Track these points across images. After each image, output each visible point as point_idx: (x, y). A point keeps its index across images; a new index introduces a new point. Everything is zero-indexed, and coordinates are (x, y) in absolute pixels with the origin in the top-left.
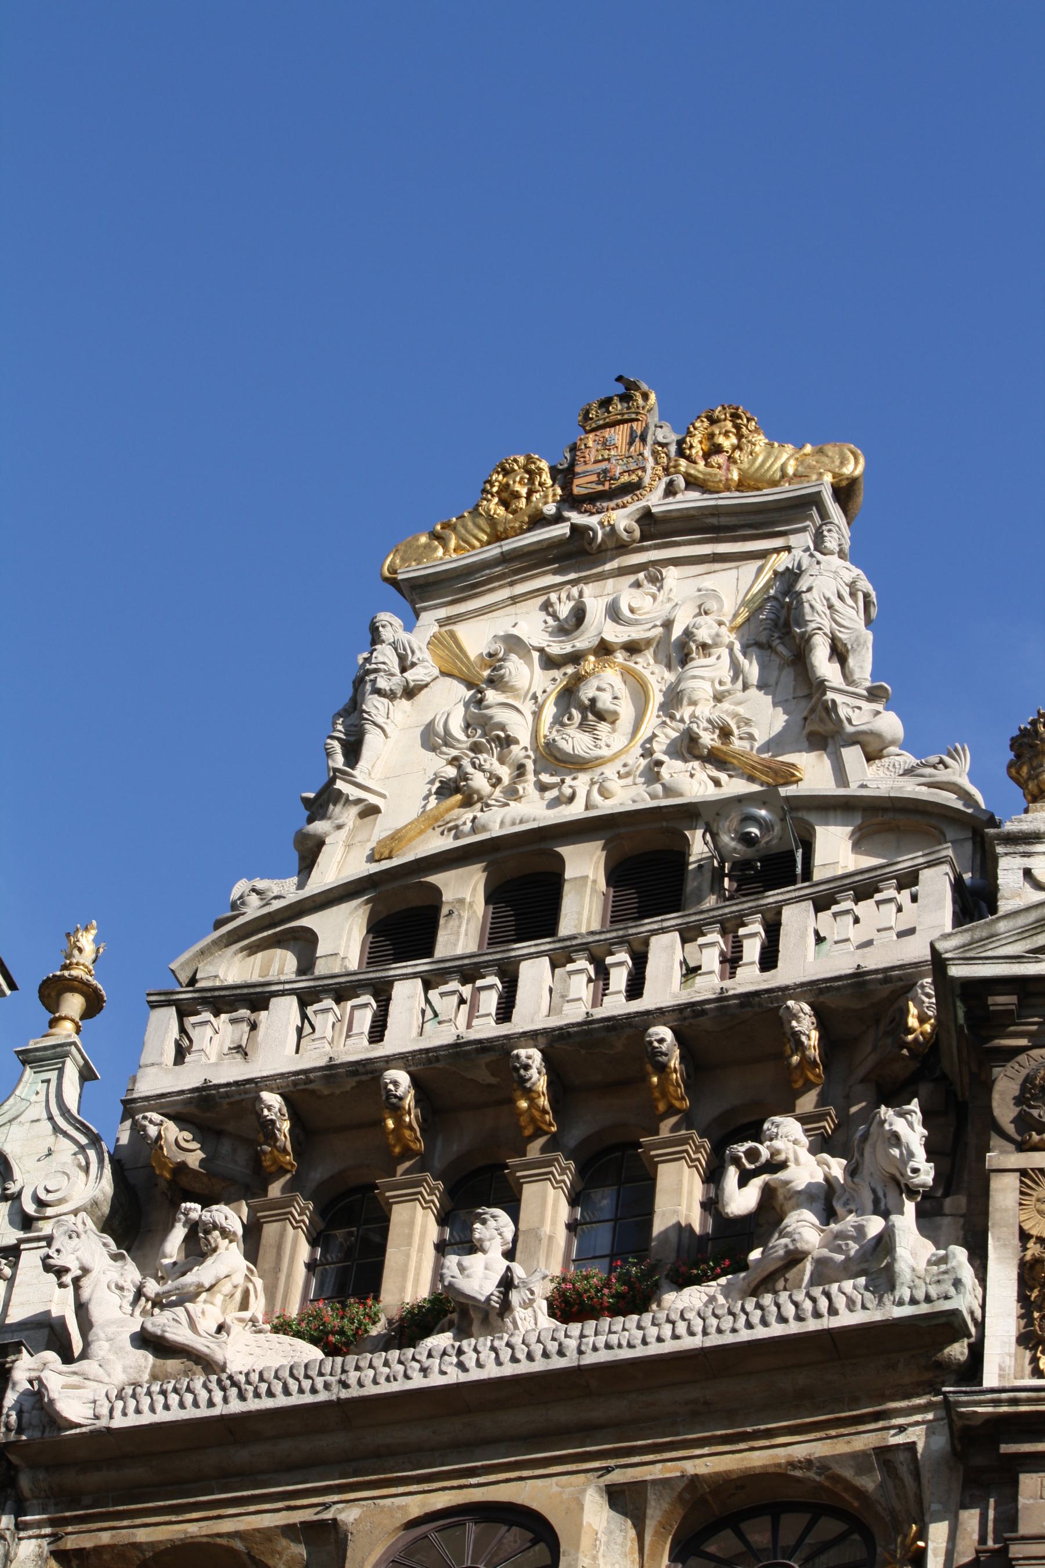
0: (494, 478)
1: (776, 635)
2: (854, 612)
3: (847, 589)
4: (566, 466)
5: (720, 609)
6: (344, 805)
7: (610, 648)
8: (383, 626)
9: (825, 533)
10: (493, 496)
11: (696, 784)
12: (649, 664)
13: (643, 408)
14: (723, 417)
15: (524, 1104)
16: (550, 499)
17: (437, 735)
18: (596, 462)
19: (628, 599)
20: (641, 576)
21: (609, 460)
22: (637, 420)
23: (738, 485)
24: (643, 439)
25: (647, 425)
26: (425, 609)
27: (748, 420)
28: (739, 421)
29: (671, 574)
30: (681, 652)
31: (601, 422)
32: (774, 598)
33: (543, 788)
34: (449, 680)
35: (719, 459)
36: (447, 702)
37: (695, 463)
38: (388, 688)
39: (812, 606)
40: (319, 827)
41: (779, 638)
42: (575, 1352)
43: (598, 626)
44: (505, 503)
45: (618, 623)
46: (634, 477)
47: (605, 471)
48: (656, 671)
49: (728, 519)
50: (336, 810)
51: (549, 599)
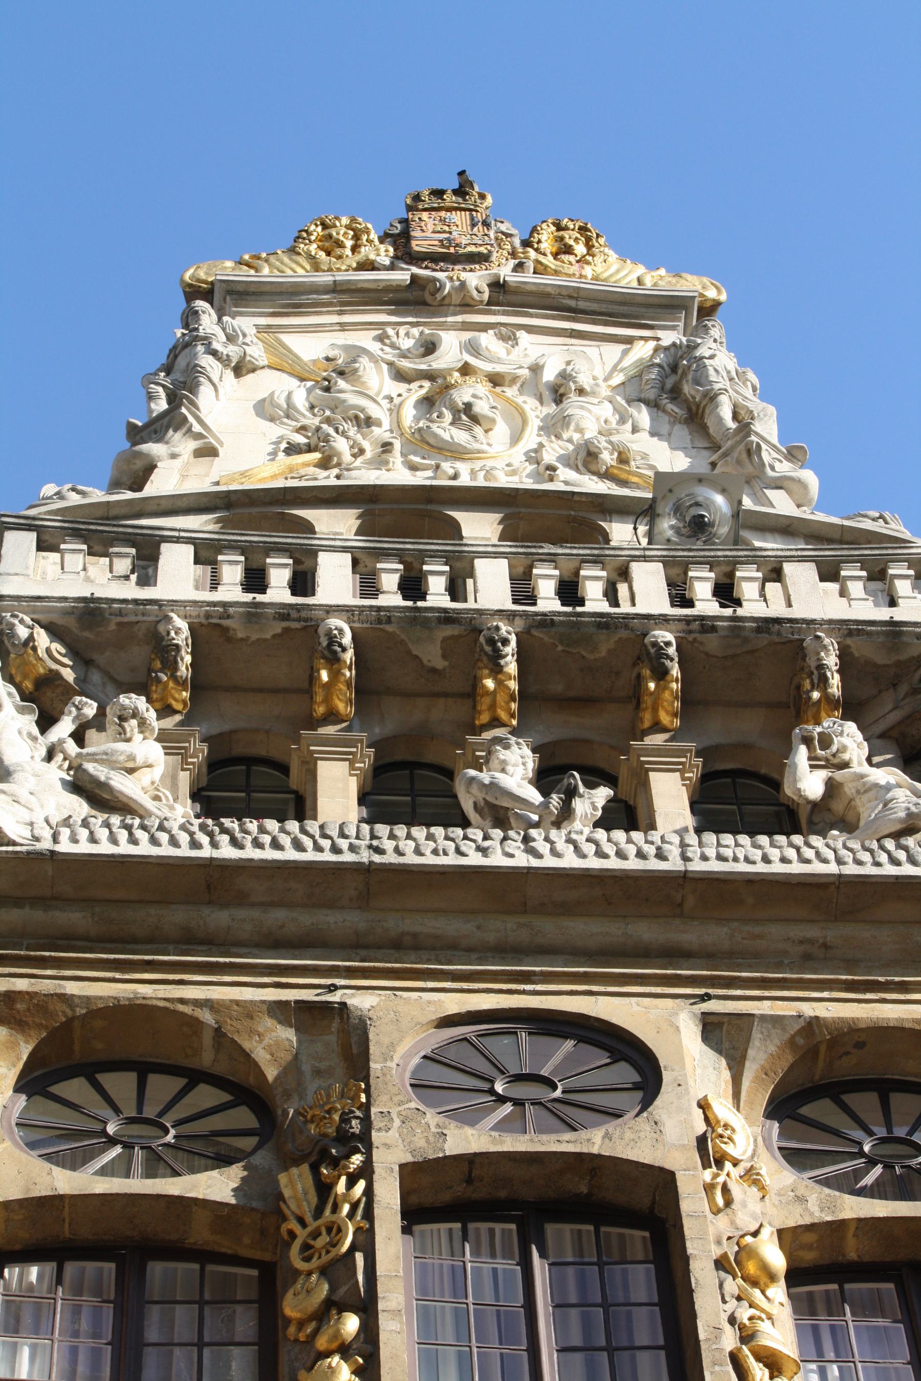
6: (184, 435)
14: (572, 227)
15: (490, 684)
17: (279, 407)
18: (434, 232)
32: (659, 365)
39: (716, 370)
40: (153, 448)
42: (678, 858)
47: (448, 239)
49: (588, 304)
50: (176, 437)
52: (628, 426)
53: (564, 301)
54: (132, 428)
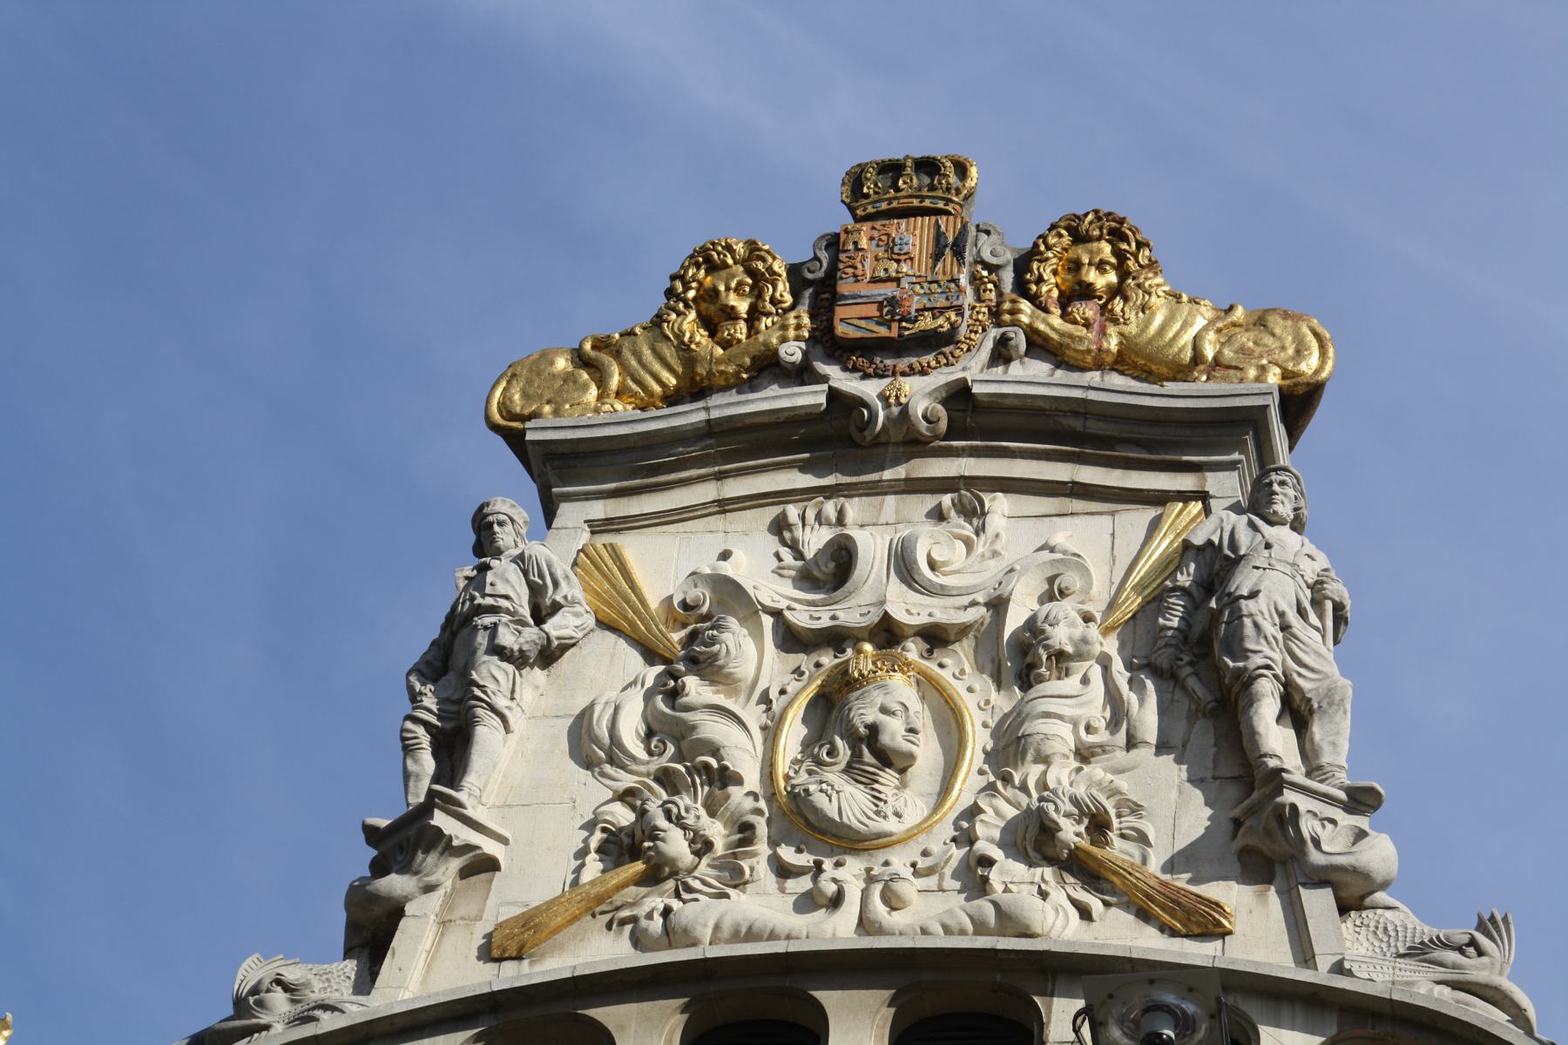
0: (690, 273)
1: (1186, 658)
2: (1317, 636)
3: (1308, 592)
4: (820, 274)
5: (1086, 590)
6: (442, 854)
7: (897, 631)
8: (501, 524)
9: (1276, 487)
10: (687, 306)
11: (1057, 918)
12: (962, 672)
13: (958, 192)
14: (1096, 233)
16: (791, 333)
17: (596, 740)
18: (875, 280)
19: (931, 543)
20: (947, 500)
21: (898, 280)
22: (948, 213)
23: (1116, 362)
24: (959, 253)
25: (964, 226)
26: (569, 498)
27: (1140, 245)
28: (1124, 246)
29: (999, 505)
30: (1024, 661)
31: (884, 206)
33: (784, 871)
34: (611, 637)
35: (1088, 310)
36: (612, 679)
37: (1046, 310)
38: (516, 648)
39: (1256, 625)
40: (395, 884)
41: (1191, 664)
43: (875, 590)
44: (710, 325)
45: (910, 586)
46: (941, 321)
47: (893, 302)
48: (977, 687)
49: (1101, 425)
51: (784, 515)
52: (1121, 737)
53: (1065, 422)
54: (373, 835)
